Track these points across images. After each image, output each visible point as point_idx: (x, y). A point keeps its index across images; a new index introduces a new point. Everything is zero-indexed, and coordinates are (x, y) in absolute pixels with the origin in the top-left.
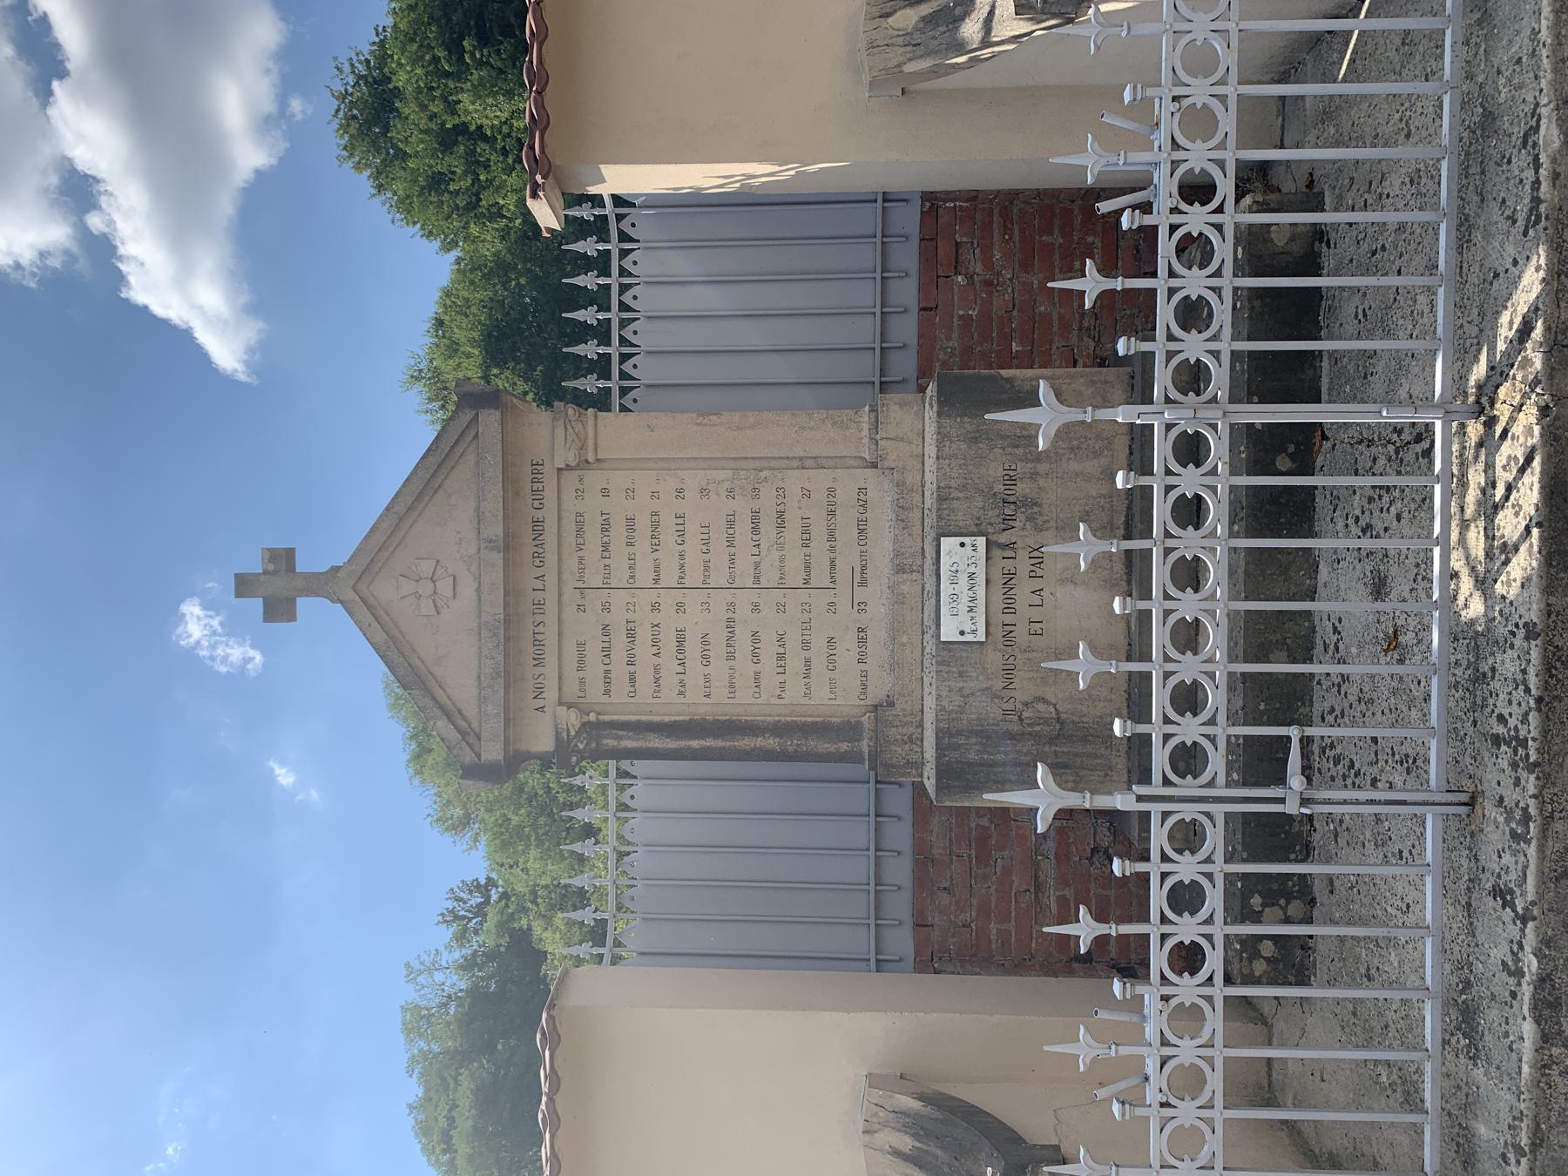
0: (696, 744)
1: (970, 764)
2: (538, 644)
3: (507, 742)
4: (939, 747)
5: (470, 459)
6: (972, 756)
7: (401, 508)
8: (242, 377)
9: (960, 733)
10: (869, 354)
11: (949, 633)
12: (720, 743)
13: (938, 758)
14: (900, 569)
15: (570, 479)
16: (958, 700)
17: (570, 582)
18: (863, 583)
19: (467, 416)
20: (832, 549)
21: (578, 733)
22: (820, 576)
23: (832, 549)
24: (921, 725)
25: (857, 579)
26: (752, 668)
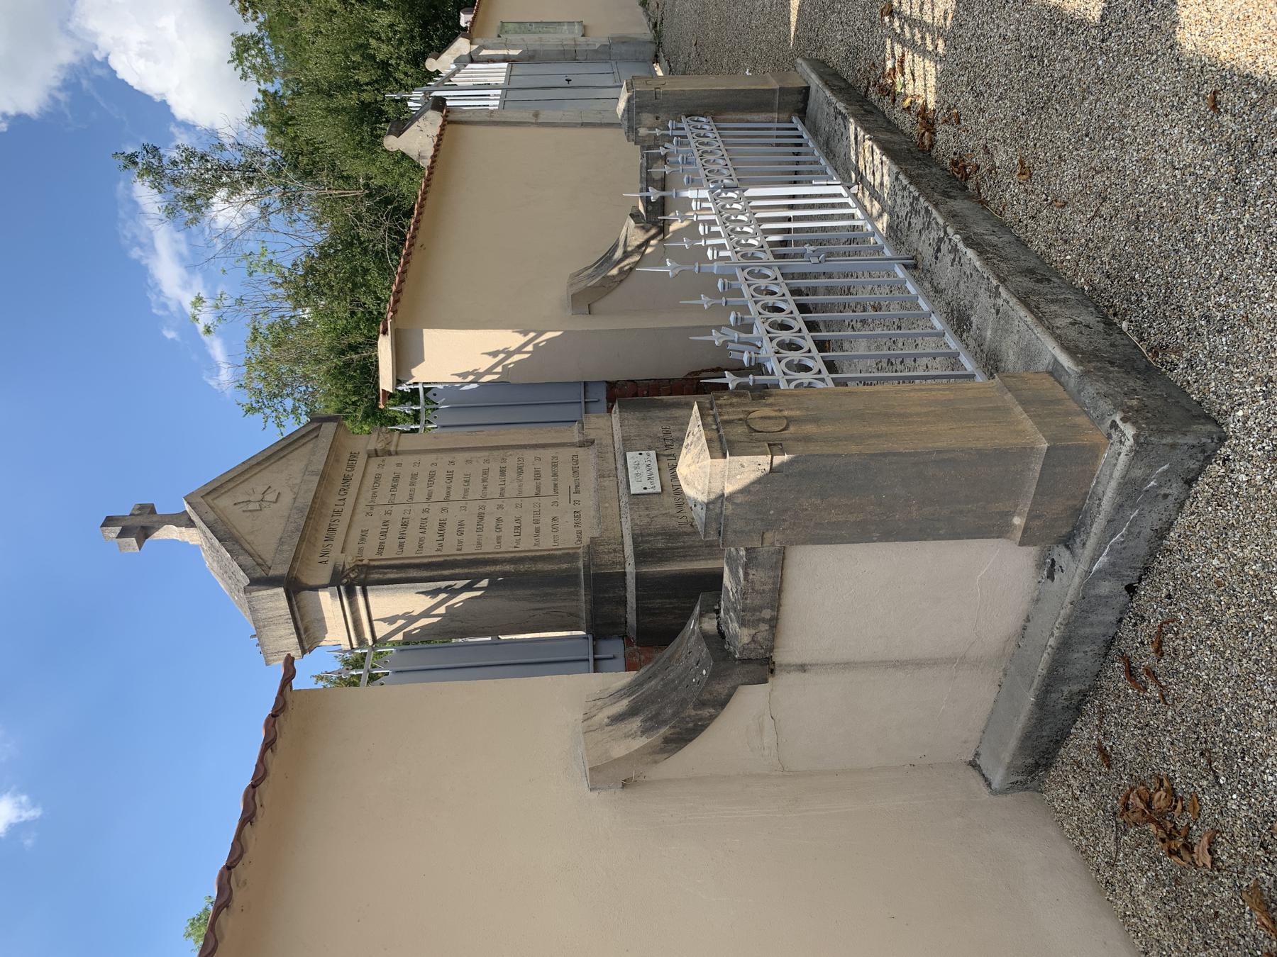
0: (446, 572)
1: (660, 550)
2: (331, 529)
3: (292, 568)
4: (634, 542)
5: (310, 445)
6: (660, 545)
7: (254, 462)
8: (35, 813)
9: (649, 535)
10: (577, 406)
11: (636, 488)
12: (466, 571)
13: (635, 548)
14: (601, 476)
15: (375, 462)
16: (646, 520)
17: (363, 502)
18: (577, 492)
19: (316, 425)
20: (555, 475)
21: (352, 570)
22: (547, 487)
23: (555, 475)
24: (622, 543)
25: (573, 490)
26: (495, 535)
